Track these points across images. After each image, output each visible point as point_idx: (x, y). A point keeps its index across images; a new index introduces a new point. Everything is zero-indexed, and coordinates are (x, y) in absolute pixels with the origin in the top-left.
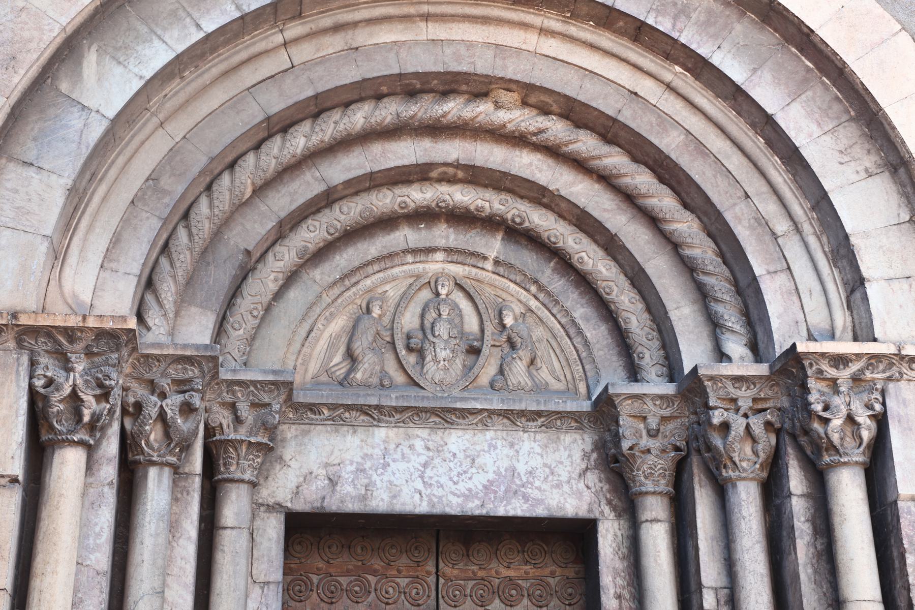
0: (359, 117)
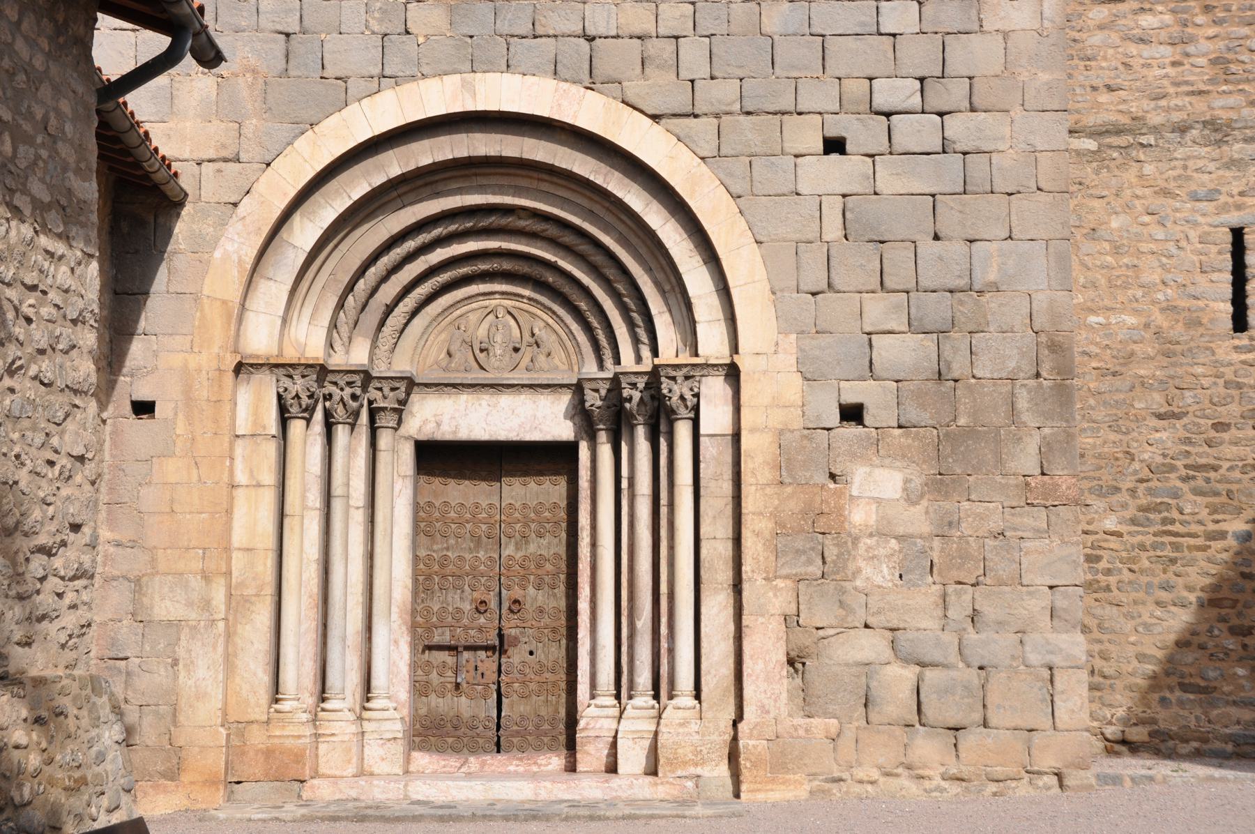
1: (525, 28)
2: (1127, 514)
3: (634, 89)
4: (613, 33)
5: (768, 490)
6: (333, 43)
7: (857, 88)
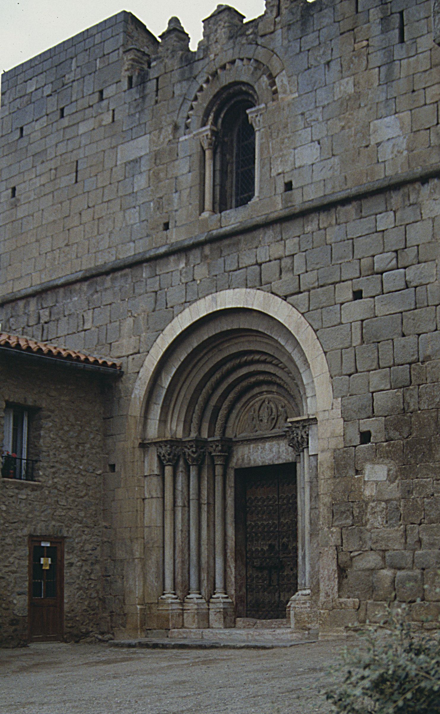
0: (229, 366)
1: (235, 268)
3: (275, 285)
4: (268, 260)
5: (329, 482)
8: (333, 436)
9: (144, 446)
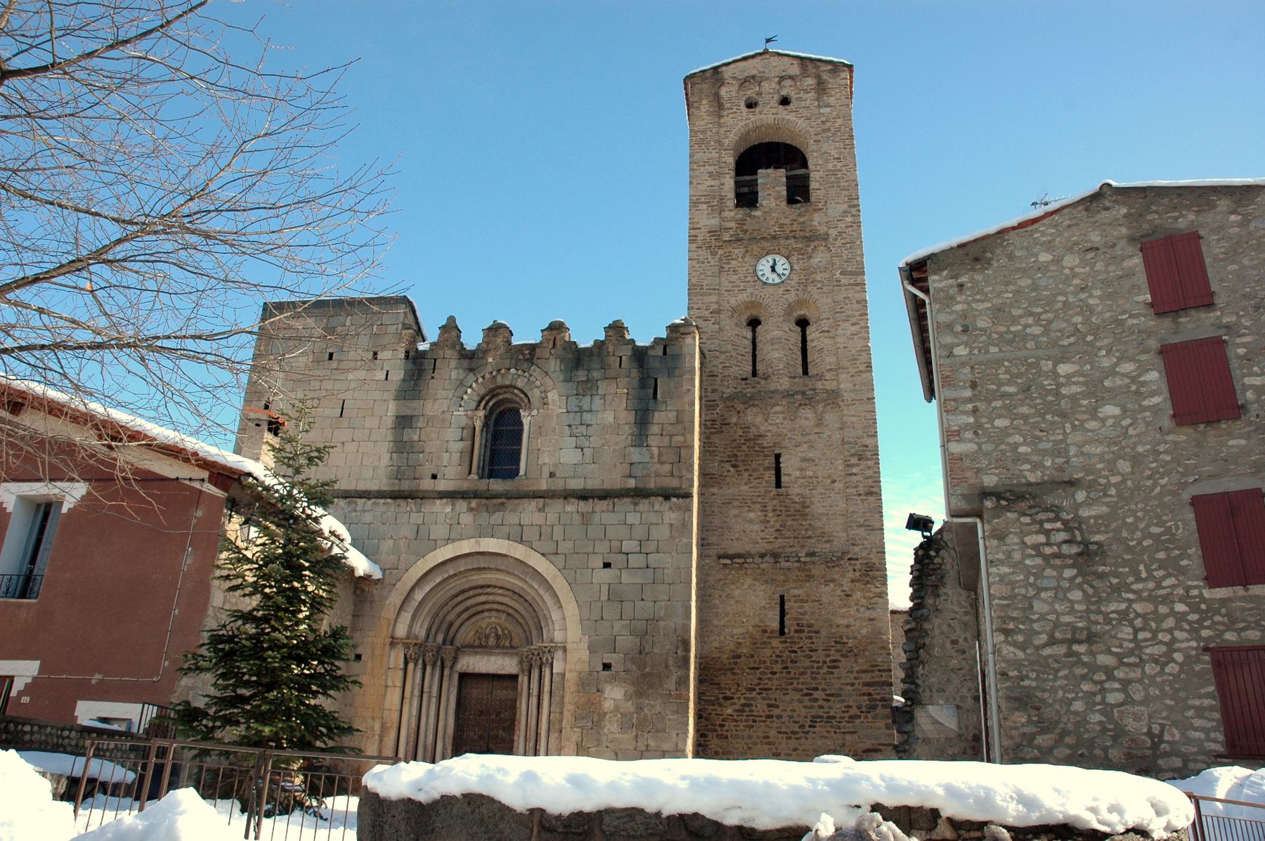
2: (737, 707)
6: (433, 527)
7: (615, 544)
8: (580, 661)
9: (394, 642)
